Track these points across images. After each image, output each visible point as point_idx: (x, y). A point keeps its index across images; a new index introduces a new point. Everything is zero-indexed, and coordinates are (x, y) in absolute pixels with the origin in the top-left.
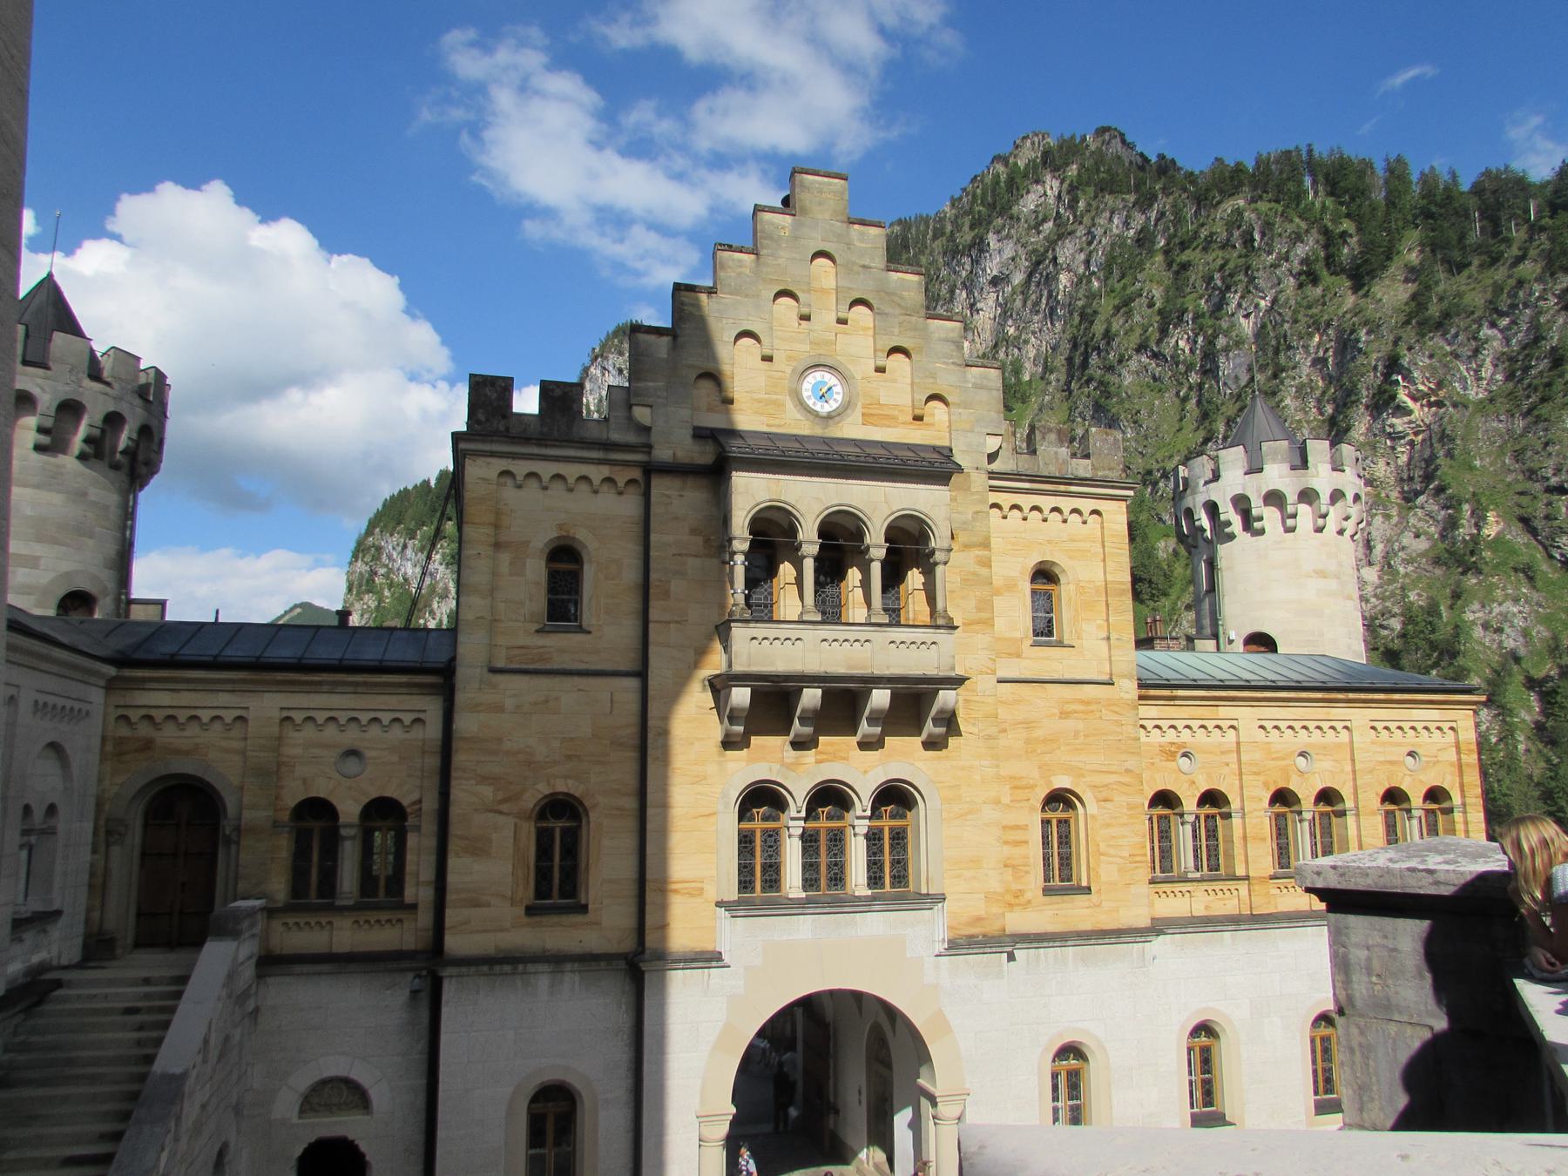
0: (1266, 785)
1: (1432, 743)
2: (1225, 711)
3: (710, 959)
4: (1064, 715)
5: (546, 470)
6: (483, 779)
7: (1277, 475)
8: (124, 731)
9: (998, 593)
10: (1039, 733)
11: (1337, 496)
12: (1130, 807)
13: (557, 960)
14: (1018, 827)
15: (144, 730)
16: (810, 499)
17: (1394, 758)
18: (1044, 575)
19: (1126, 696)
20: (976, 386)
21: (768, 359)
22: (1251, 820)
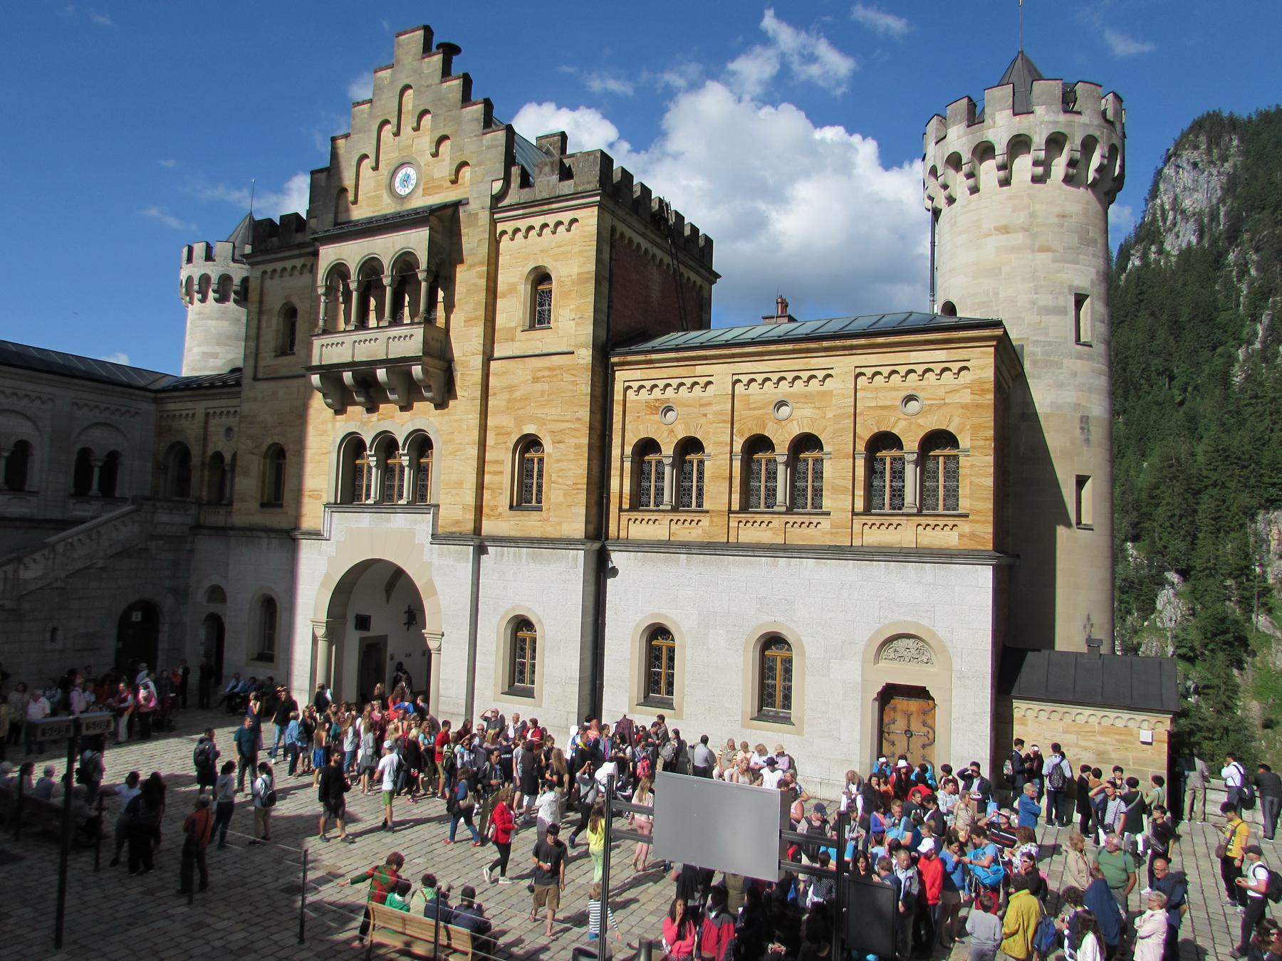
0: (741, 432)
2: (700, 370)
3: (316, 535)
4: (536, 380)
5: (279, 266)
7: (959, 139)
9: (504, 296)
10: (517, 394)
11: (1019, 144)
12: (577, 447)
13: (268, 530)
14: (497, 462)
17: (888, 403)
18: (541, 277)
20: (489, 148)
22: (719, 464)
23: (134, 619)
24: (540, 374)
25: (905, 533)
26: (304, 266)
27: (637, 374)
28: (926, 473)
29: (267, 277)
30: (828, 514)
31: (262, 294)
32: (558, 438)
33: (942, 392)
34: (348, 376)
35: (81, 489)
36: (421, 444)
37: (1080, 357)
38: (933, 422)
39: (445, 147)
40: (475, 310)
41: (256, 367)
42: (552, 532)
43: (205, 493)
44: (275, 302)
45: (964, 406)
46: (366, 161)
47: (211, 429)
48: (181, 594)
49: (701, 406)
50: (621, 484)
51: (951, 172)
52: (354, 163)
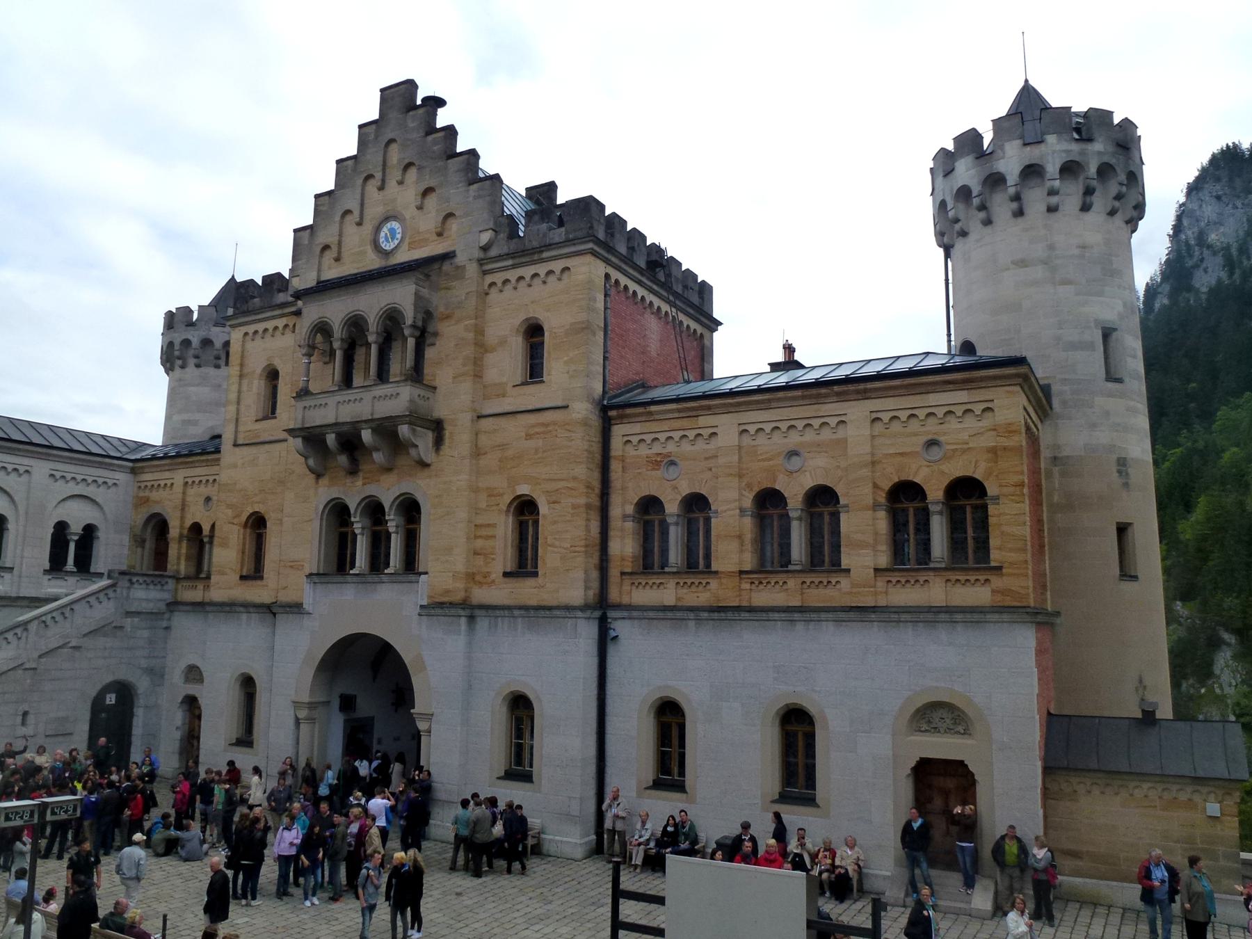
0: (749, 486)
1: (955, 432)
2: (703, 421)
3: (296, 608)
4: (529, 437)
5: (260, 327)
6: (229, 506)
8: (142, 494)
10: (510, 453)
11: (1032, 172)
12: (574, 507)
13: (248, 607)
14: (489, 525)
15: (147, 493)
16: (335, 310)
17: (908, 450)
18: (534, 332)
19: (580, 416)
20: (475, 198)
21: (359, 224)
23: (108, 702)
24: (532, 431)
25: (935, 592)
26: (286, 326)
27: (637, 428)
28: (956, 526)
29: (248, 338)
30: (848, 571)
31: (242, 357)
32: (554, 498)
33: (964, 436)
34: (331, 439)
35: (56, 564)
36: (410, 509)
37: (1111, 395)
38: (957, 469)
39: (431, 201)
40: (464, 365)
41: (236, 432)
42: (547, 598)
43: (182, 567)
44: (257, 365)
45: (993, 451)
46: (348, 218)
47: (188, 499)
48: (157, 674)
49: (706, 459)
50: (624, 545)
51: (961, 206)
52: (337, 218)
